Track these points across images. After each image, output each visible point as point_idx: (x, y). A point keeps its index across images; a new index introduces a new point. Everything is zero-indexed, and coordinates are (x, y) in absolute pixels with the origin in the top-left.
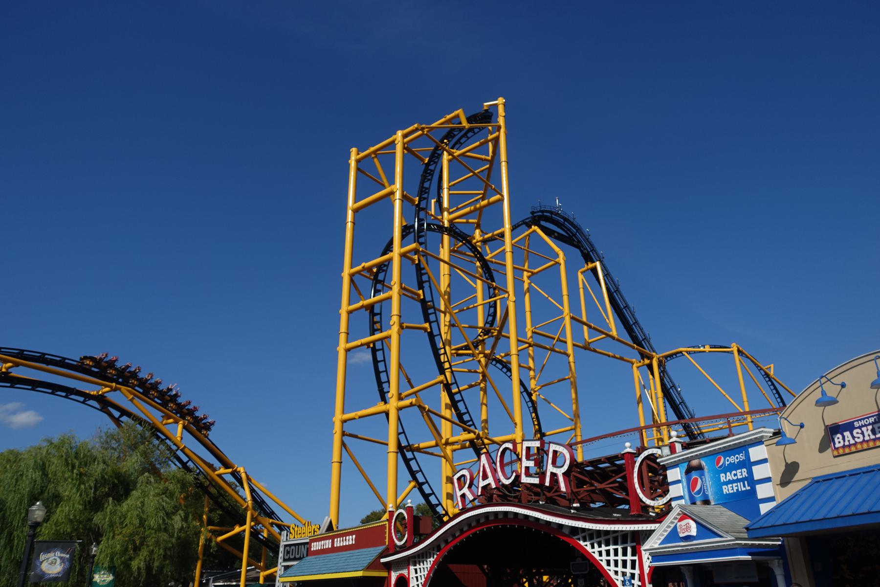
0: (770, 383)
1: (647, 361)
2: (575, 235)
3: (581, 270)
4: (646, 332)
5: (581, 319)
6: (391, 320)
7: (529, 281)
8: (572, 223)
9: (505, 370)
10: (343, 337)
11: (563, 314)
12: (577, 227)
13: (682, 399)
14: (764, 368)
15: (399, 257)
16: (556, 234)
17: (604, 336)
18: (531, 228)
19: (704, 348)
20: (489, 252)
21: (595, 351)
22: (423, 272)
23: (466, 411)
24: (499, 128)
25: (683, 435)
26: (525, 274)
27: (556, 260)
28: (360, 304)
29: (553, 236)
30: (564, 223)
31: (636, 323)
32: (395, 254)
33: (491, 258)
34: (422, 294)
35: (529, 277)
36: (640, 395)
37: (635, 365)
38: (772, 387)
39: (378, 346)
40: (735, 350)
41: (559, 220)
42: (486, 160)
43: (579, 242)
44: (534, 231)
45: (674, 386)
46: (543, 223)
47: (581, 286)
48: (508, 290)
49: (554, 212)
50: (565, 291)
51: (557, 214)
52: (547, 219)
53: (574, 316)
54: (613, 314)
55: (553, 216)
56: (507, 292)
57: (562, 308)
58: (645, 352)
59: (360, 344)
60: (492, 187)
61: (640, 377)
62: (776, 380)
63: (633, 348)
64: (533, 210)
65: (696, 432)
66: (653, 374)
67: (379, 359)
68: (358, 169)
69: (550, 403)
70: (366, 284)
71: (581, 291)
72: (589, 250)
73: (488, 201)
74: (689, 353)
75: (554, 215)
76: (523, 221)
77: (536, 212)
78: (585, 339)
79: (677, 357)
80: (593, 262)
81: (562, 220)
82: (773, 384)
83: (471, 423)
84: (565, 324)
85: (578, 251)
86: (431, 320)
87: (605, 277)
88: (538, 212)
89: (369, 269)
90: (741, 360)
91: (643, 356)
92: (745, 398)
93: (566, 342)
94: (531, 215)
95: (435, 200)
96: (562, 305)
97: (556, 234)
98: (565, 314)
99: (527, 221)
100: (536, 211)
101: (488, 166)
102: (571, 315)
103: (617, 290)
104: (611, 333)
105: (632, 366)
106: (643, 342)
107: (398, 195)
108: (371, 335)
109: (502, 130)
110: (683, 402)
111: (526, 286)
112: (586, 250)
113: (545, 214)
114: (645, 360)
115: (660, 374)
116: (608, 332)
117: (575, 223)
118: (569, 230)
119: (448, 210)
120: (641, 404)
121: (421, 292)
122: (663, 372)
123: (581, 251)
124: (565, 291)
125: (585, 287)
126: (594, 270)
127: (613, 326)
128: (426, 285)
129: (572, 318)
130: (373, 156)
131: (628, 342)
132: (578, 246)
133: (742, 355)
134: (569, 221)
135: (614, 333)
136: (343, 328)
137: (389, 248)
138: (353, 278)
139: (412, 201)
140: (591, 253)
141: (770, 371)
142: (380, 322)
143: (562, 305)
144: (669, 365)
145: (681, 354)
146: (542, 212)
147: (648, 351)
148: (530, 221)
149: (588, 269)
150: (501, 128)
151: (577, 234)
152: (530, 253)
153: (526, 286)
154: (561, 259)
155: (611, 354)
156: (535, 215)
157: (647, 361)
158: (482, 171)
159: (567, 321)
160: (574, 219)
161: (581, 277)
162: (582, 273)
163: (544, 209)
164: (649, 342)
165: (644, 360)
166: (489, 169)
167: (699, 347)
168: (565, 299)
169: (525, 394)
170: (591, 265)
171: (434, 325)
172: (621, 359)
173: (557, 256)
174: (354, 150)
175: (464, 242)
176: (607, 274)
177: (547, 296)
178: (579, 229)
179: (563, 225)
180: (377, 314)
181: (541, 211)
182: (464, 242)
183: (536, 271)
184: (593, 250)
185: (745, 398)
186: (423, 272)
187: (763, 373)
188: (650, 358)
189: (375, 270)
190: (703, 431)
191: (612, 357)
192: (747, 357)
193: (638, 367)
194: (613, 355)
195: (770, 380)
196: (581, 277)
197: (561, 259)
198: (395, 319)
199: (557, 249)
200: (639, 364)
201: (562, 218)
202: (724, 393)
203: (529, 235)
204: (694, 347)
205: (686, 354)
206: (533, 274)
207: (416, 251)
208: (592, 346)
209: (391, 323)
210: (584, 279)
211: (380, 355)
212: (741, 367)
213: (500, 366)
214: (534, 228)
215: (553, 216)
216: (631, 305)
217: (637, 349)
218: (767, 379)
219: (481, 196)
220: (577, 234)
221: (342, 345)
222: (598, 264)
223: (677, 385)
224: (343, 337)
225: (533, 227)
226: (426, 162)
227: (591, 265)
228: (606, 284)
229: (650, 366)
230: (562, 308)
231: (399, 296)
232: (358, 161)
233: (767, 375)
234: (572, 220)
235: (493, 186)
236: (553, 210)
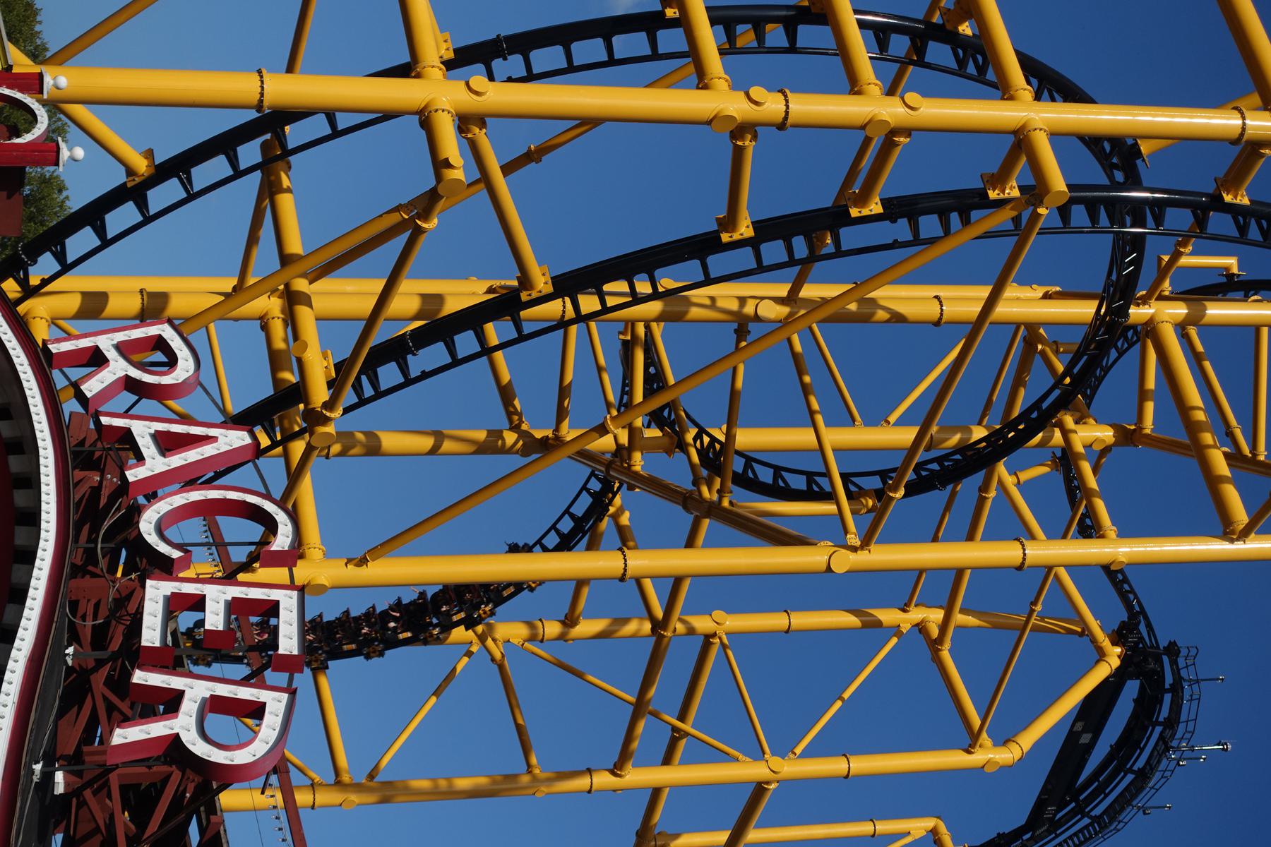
2: (1080, 811)
3: (943, 828)
6: (769, 90)
7: (905, 628)
8: (1129, 803)
9: (566, 525)
11: (774, 754)
12: (1111, 821)
16: (1085, 739)
18: (1114, 643)
20: (1025, 476)
26: (936, 615)
27: (984, 735)
29: (1079, 726)
30: (1131, 770)
33: (1000, 482)
35: (921, 627)
39: (670, 40)
41: (1142, 750)
43: (1055, 826)
44: (1101, 655)
46: (1132, 688)
49: (1173, 736)
50: (863, 764)
51: (1164, 745)
55: (1159, 729)
57: (798, 750)
64: (1184, 652)
75: (1161, 737)
76: (1143, 612)
77: (1174, 663)
78: (677, 836)
81: (1140, 764)
84: (737, 760)
86: (764, 248)
88: (1176, 671)
93: (667, 761)
94: (1163, 643)
95: (1235, 270)
96: (808, 754)
97: (1085, 739)
98: (775, 762)
99: (1142, 628)
102: (773, 786)
108: (708, 8)
111: (888, 616)
113: (1167, 698)
118: (1101, 791)
124: (863, 764)
129: (759, 789)
134: (1140, 790)
142: (762, 48)
143: (807, 754)
146: (1177, 689)
148: (1141, 639)
151: (1086, 821)
152: (1018, 633)
153: (888, 616)
154: (989, 755)
156: (1165, 659)
159: (748, 770)
161: (919, 827)
162: (934, 832)
163: (1187, 696)
168: (834, 766)
173: (1003, 740)
177: (846, 695)
178: (1103, 827)
179: (1121, 769)
180: (792, 35)
181: (1178, 680)
183: (946, 655)
197: (989, 755)
198: (772, 105)
199: (1028, 739)
201: (1148, 762)
203: (1086, 632)
206: (935, 645)
209: (756, 92)
211: (630, 44)
213: (580, 509)
214: (1114, 656)
215: (1159, 729)
220: (1086, 821)
225: (1118, 650)
230: (798, 750)
231: (861, 122)
234: (1139, 801)
236: (1181, 729)
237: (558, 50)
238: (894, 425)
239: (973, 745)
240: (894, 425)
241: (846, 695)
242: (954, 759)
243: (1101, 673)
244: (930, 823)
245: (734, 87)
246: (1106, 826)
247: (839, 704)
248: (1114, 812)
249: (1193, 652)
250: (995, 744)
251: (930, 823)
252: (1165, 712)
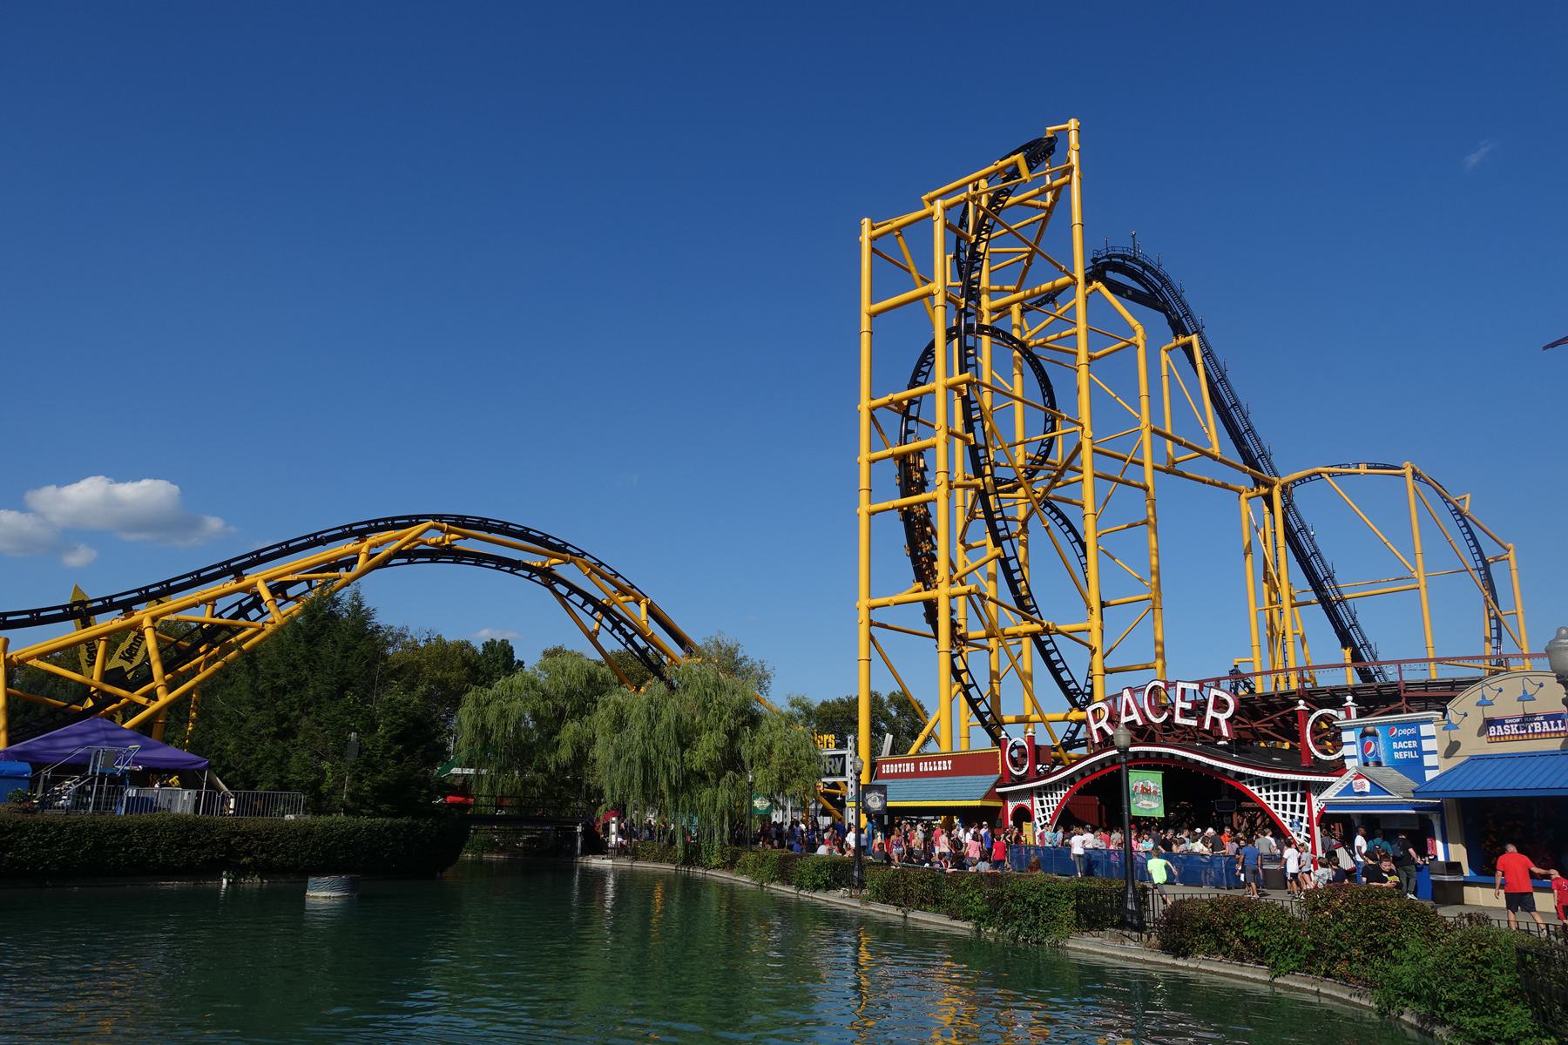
0: (1461, 523)
1: (1264, 490)
3: (1166, 347)
4: (1265, 444)
5: (1163, 431)
10: (864, 495)
12: (1164, 278)
13: (1315, 547)
14: (1454, 500)
15: (944, 389)
16: (1130, 293)
17: (1197, 454)
19: (1358, 468)
21: (1182, 475)
22: (973, 406)
24: (1069, 170)
25: (1313, 601)
27: (1130, 340)
28: (889, 451)
29: (1124, 295)
30: (1143, 272)
31: (1250, 429)
32: (939, 382)
34: (973, 439)
36: (1250, 542)
37: (1243, 496)
38: (1465, 530)
40: (1408, 472)
42: (1042, 207)
43: (1166, 302)
45: (1304, 528)
46: (1110, 274)
47: (1165, 372)
48: (1080, 421)
50: (1144, 390)
51: (1134, 260)
53: (1157, 428)
54: (1214, 416)
55: (1126, 262)
56: (1081, 425)
57: (1138, 416)
58: (1264, 478)
59: (891, 507)
60: (1061, 268)
61: (1251, 513)
62: (1470, 518)
63: (1244, 471)
64: (1095, 256)
65: (1333, 598)
66: (1272, 511)
68: (873, 250)
69: (1114, 559)
70: (893, 421)
71: (1165, 379)
73: (1053, 285)
74: (1332, 475)
77: (1100, 259)
78: (1168, 454)
79: (1311, 480)
80: (1186, 334)
81: (1140, 268)
82: (1466, 525)
87: (1205, 358)
88: (1103, 258)
89: (899, 403)
90: (1418, 489)
91: (1258, 482)
92: (1418, 549)
93: (1142, 464)
94: (1092, 264)
97: (1130, 293)
98: (1143, 425)
100: (1099, 256)
101: (1044, 215)
103: (1223, 379)
104: (1209, 450)
105: (1239, 497)
106: (1259, 460)
107: (939, 299)
108: (902, 498)
109: (1076, 173)
110: (1317, 552)
112: (1176, 316)
113: (1113, 260)
114: (1261, 487)
115: (1283, 509)
116: (1202, 448)
119: (990, 292)
120: (1249, 556)
121: (971, 435)
122: (1288, 506)
123: (1168, 317)
124: (1144, 390)
125: (1170, 375)
126: (1188, 348)
127: (1213, 437)
128: (977, 425)
129: (1154, 431)
130: (897, 233)
131: (1237, 464)
132: (1163, 307)
133: (1419, 480)
135: (1216, 450)
136: (864, 483)
137: (922, 369)
138: (874, 413)
139: (957, 305)
140: (1184, 319)
141: (1464, 506)
143: (1140, 413)
144: (1298, 494)
145: (1319, 477)
147: (1267, 476)
149: (1177, 346)
150: (1072, 170)
151: (1164, 289)
154: (1139, 338)
155: (1207, 479)
157: (1264, 490)
158: (1034, 222)
159: (1146, 436)
160: (1159, 266)
161: (1165, 357)
162: (1166, 351)
164: (1269, 461)
165: (1258, 488)
166: (1045, 219)
167: (1349, 467)
168: (1144, 402)
169: (1077, 545)
170: (1182, 340)
172: (1225, 486)
173: (1134, 332)
174: (866, 221)
175: (1015, 345)
176: (1207, 354)
177: (1114, 395)
181: (1107, 256)
182: (1015, 345)
185: (1418, 549)
186: (973, 406)
187: (1452, 508)
188: (1270, 485)
189: (905, 403)
190: (1346, 596)
191: (1209, 483)
192: (1428, 483)
193: (1249, 498)
194: (1211, 480)
195: (1462, 518)
196: (1165, 357)
197: (1139, 338)
198: (942, 477)
199: (1133, 322)
200: (1251, 494)
202: (1385, 541)
204: (1340, 466)
205: (1327, 477)
207: (969, 383)
208: (1178, 467)
209: (937, 482)
210: (1170, 361)
212: (1415, 497)
214: (1097, 285)
215: (1126, 262)
216: (1243, 403)
217: (1250, 473)
218: (1458, 517)
219: (1026, 255)
220: (1164, 289)
221: (864, 508)
222: (1194, 338)
223: (1309, 526)
224: (864, 495)
225: (1094, 283)
226: (973, 241)
227: (1182, 340)
228: (1206, 369)
229: (1268, 499)
230: (1138, 416)
232: (873, 239)
233: (1458, 511)
235: (1064, 267)
236: (1126, 253)
238: (1013, 387)
239: (1136, 345)
240: (1013, 387)
241: (1114, 395)
242: (1141, 352)
243: (1104, 290)
244: (1163, 352)
245: (936, 490)
246: (1165, 280)
247: (1118, 399)
248: (1160, 278)
250: (1135, 335)
251: (1163, 352)
252: (1120, 260)
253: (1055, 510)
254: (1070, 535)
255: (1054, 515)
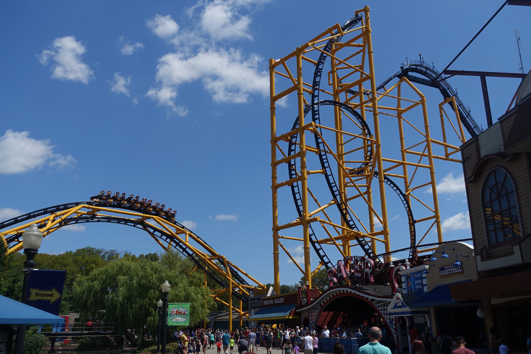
12: (436, 73)
23: (351, 219)
46: (410, 73)
52: (413, 70)
55: (418, 67)
64: (402, 66)
67: (296, 192)
72: (446, 89)
76: (395, 75)
83: (354, 226)
85: (437, 90)
86: (326, 166)
94: (401, 70)
117: (435, 70)
123: (440, 90)
134: (430, 69)
171: (328, 169)
184: (449, 88)
215: (418, 67)
237: (298, 201)
249: (402, 64)
253: (389, 180)
254: (398, 191)
255: (389, 183)
